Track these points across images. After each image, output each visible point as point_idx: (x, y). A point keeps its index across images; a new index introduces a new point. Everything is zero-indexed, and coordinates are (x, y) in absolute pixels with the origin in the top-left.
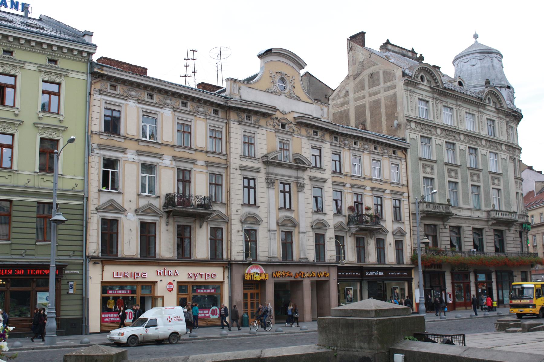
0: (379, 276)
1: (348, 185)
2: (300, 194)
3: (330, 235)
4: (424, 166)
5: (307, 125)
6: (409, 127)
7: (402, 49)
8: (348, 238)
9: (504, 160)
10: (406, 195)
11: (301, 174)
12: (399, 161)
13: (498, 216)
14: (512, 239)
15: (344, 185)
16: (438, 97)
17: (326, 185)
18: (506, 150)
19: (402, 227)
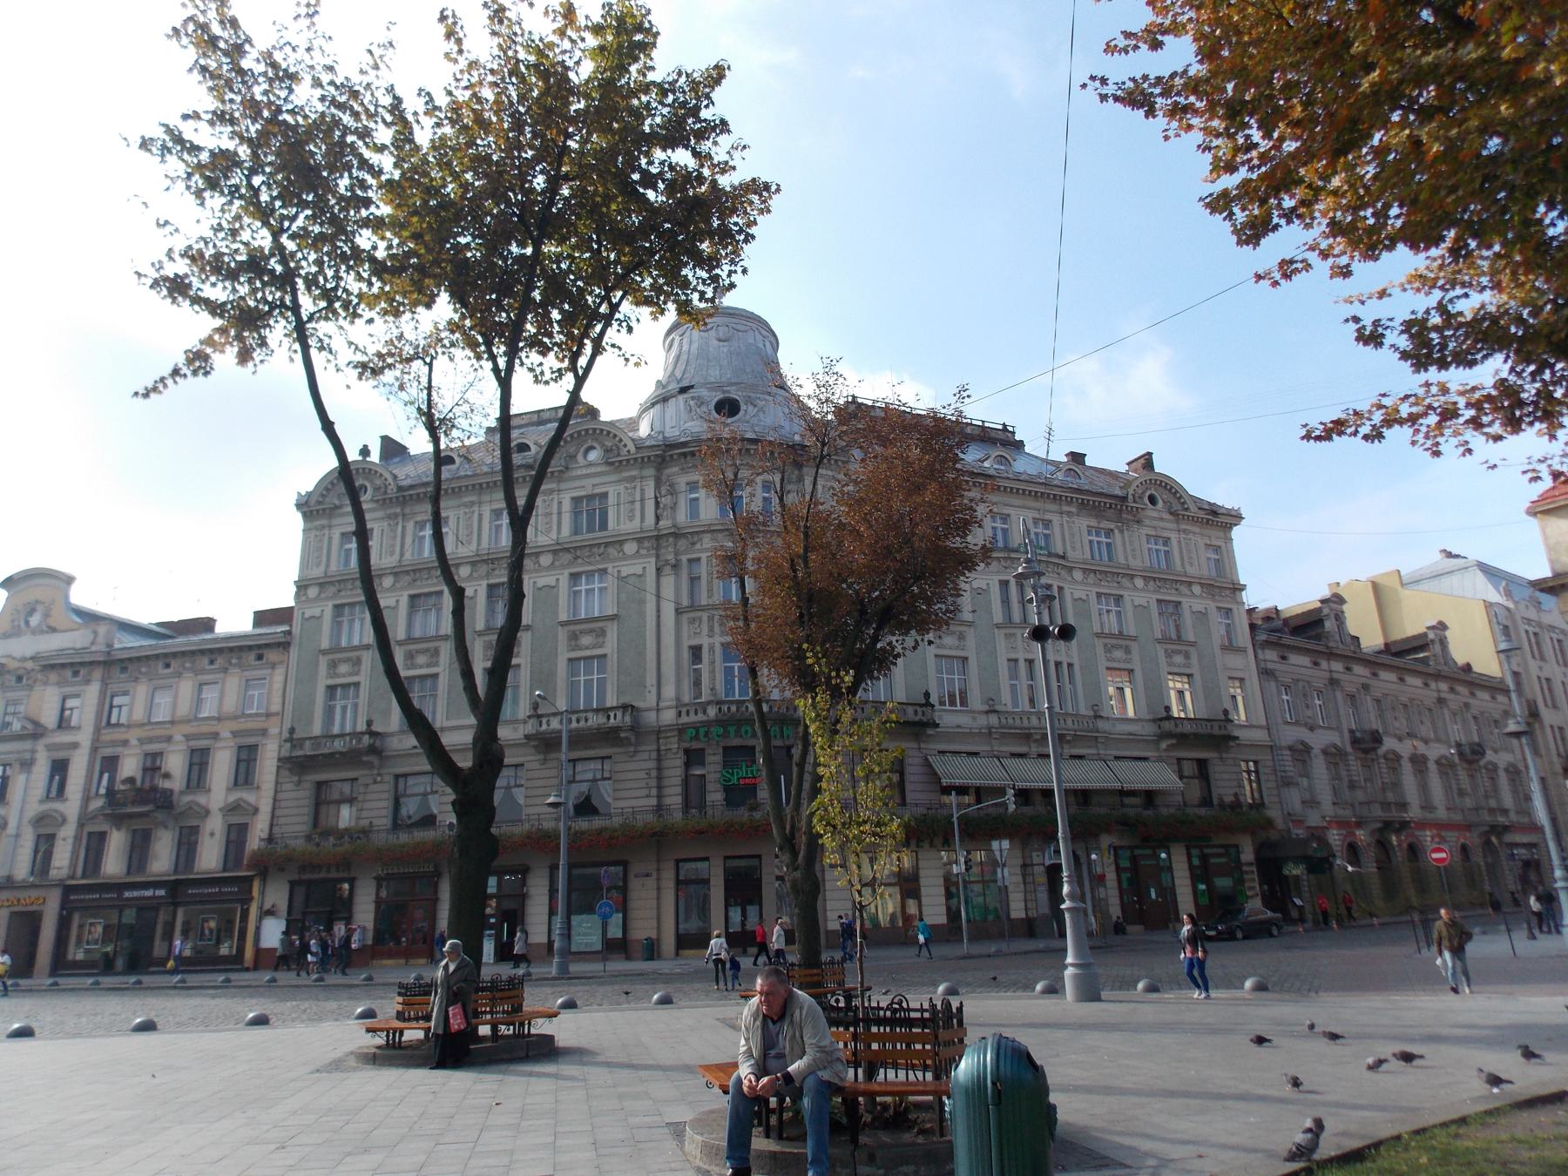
0: (154, 897)
1: (134, 742)
2: (22, 778)
3: (67, 833)
4: (333, 665)
5: (53, 667)
6: (304, 598)
7: (539, 412)
8: (114, 830)
9: (633, 578)
10: (274, 731)
11: (27, 745)
12: (269, 671)
13: (544, 727)
14: (642, 775)
15: (125, 743)
16: (398, 510)
17: (78, 752)
18: (643, 552)
19: (249, 797)
